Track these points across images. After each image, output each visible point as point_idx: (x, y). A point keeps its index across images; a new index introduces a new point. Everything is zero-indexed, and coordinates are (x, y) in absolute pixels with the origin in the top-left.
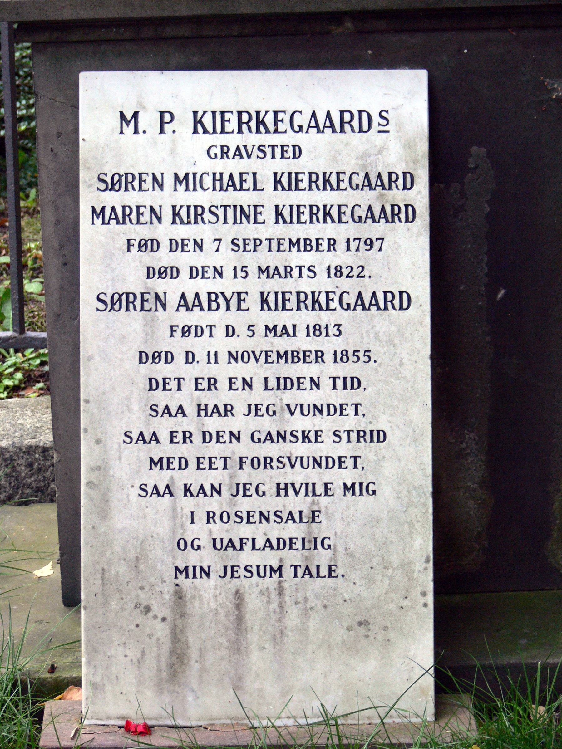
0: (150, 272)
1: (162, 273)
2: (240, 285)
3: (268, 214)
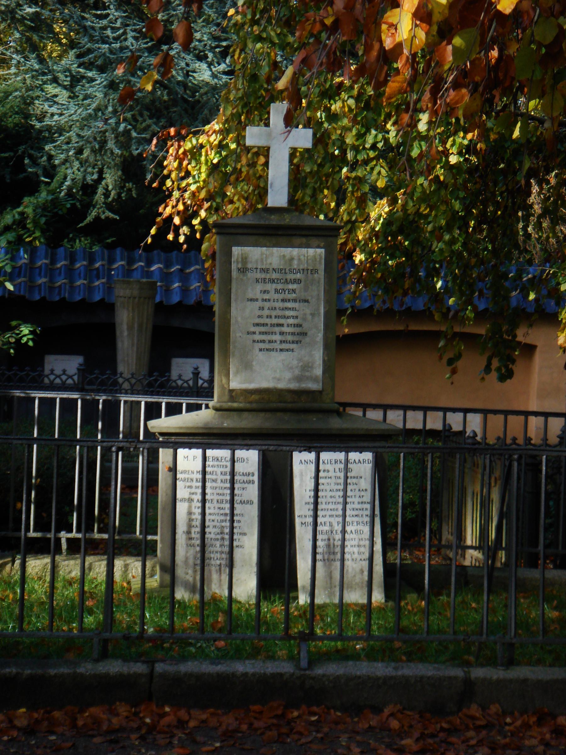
0: (191, 494)
1: (193, 494)
2: (212, 497)
3: (219, 481)
